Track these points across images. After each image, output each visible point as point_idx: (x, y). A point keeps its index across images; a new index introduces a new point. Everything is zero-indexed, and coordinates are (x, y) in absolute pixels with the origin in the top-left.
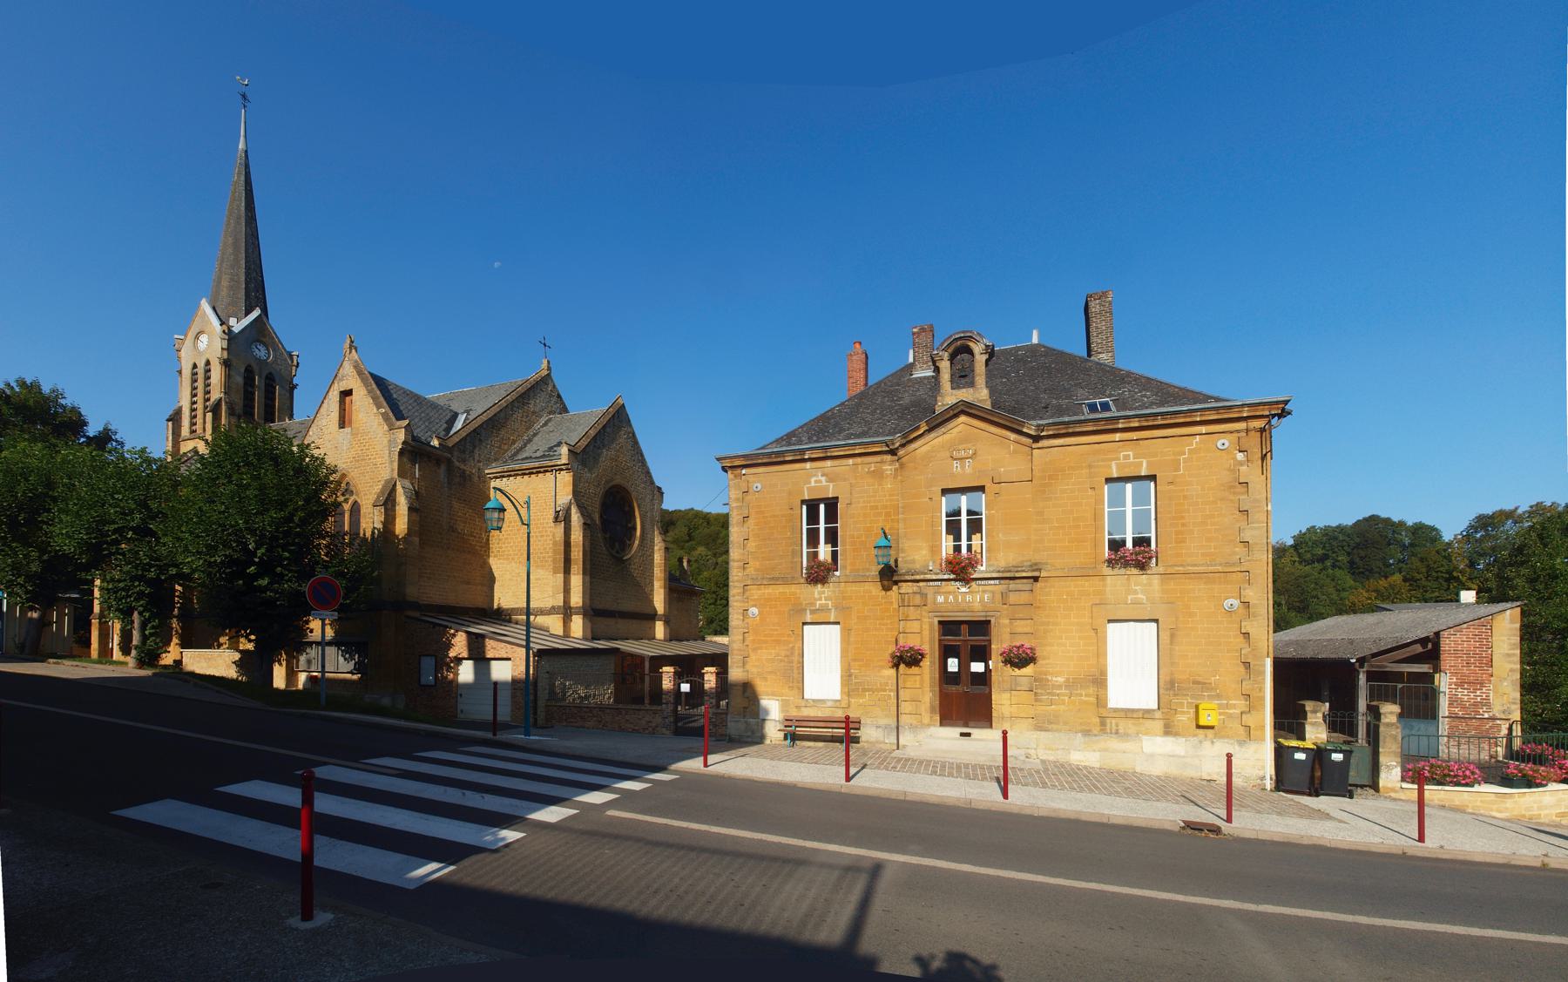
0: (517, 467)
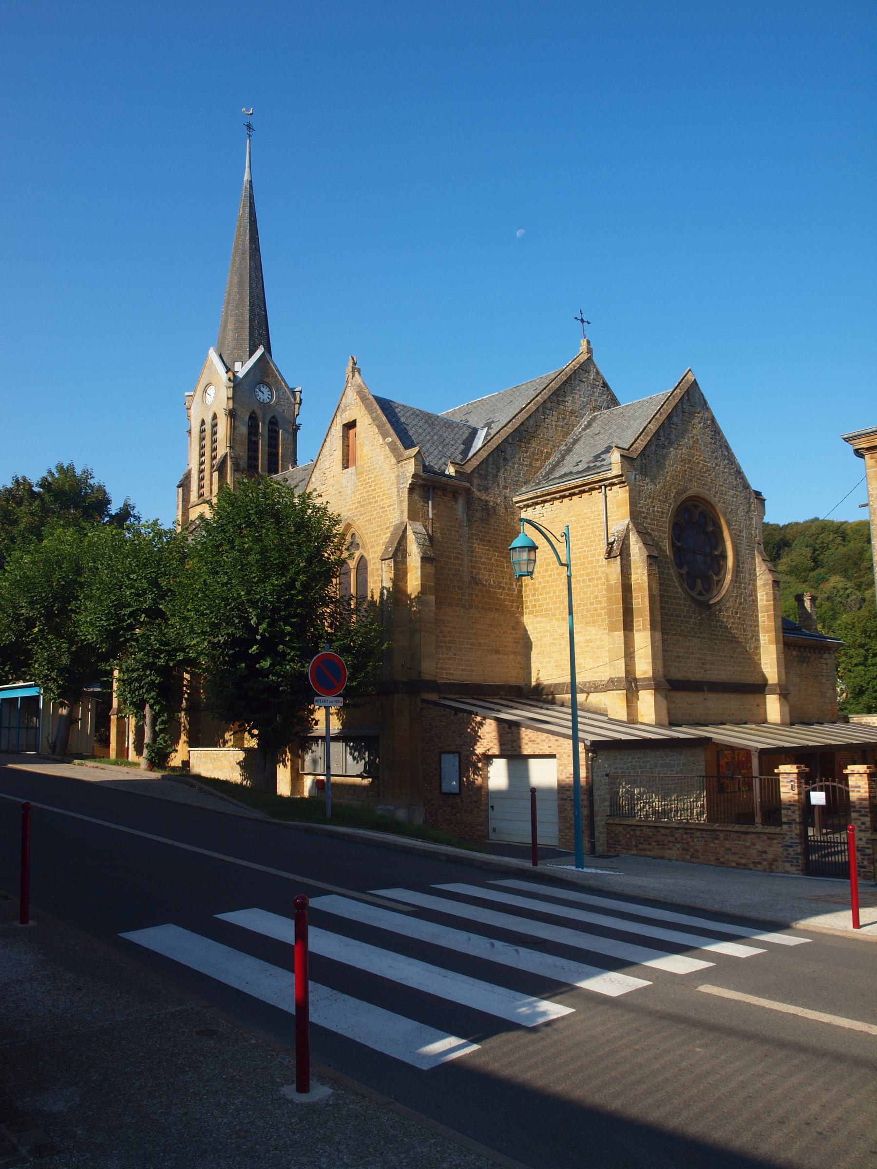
0: (553, 488)
